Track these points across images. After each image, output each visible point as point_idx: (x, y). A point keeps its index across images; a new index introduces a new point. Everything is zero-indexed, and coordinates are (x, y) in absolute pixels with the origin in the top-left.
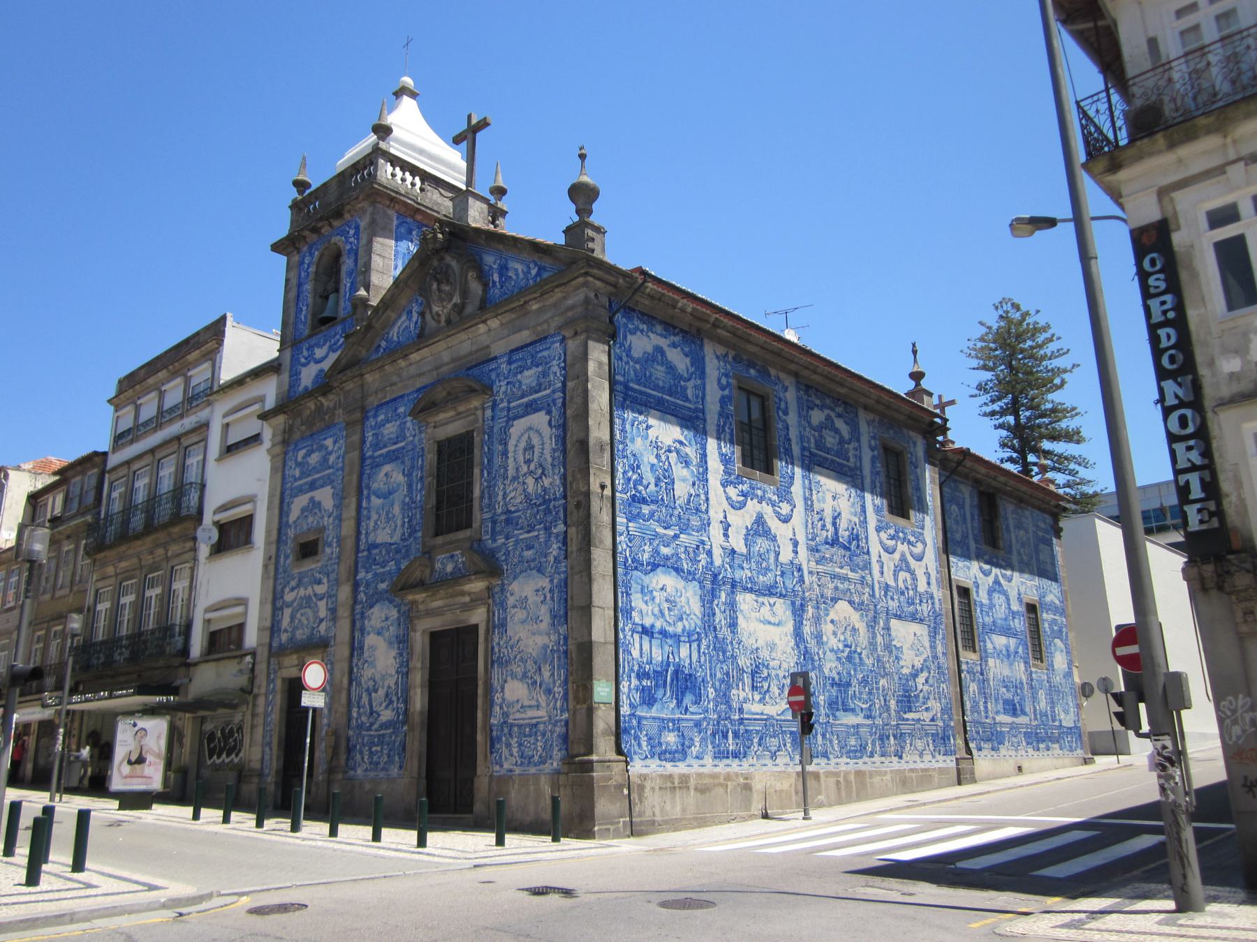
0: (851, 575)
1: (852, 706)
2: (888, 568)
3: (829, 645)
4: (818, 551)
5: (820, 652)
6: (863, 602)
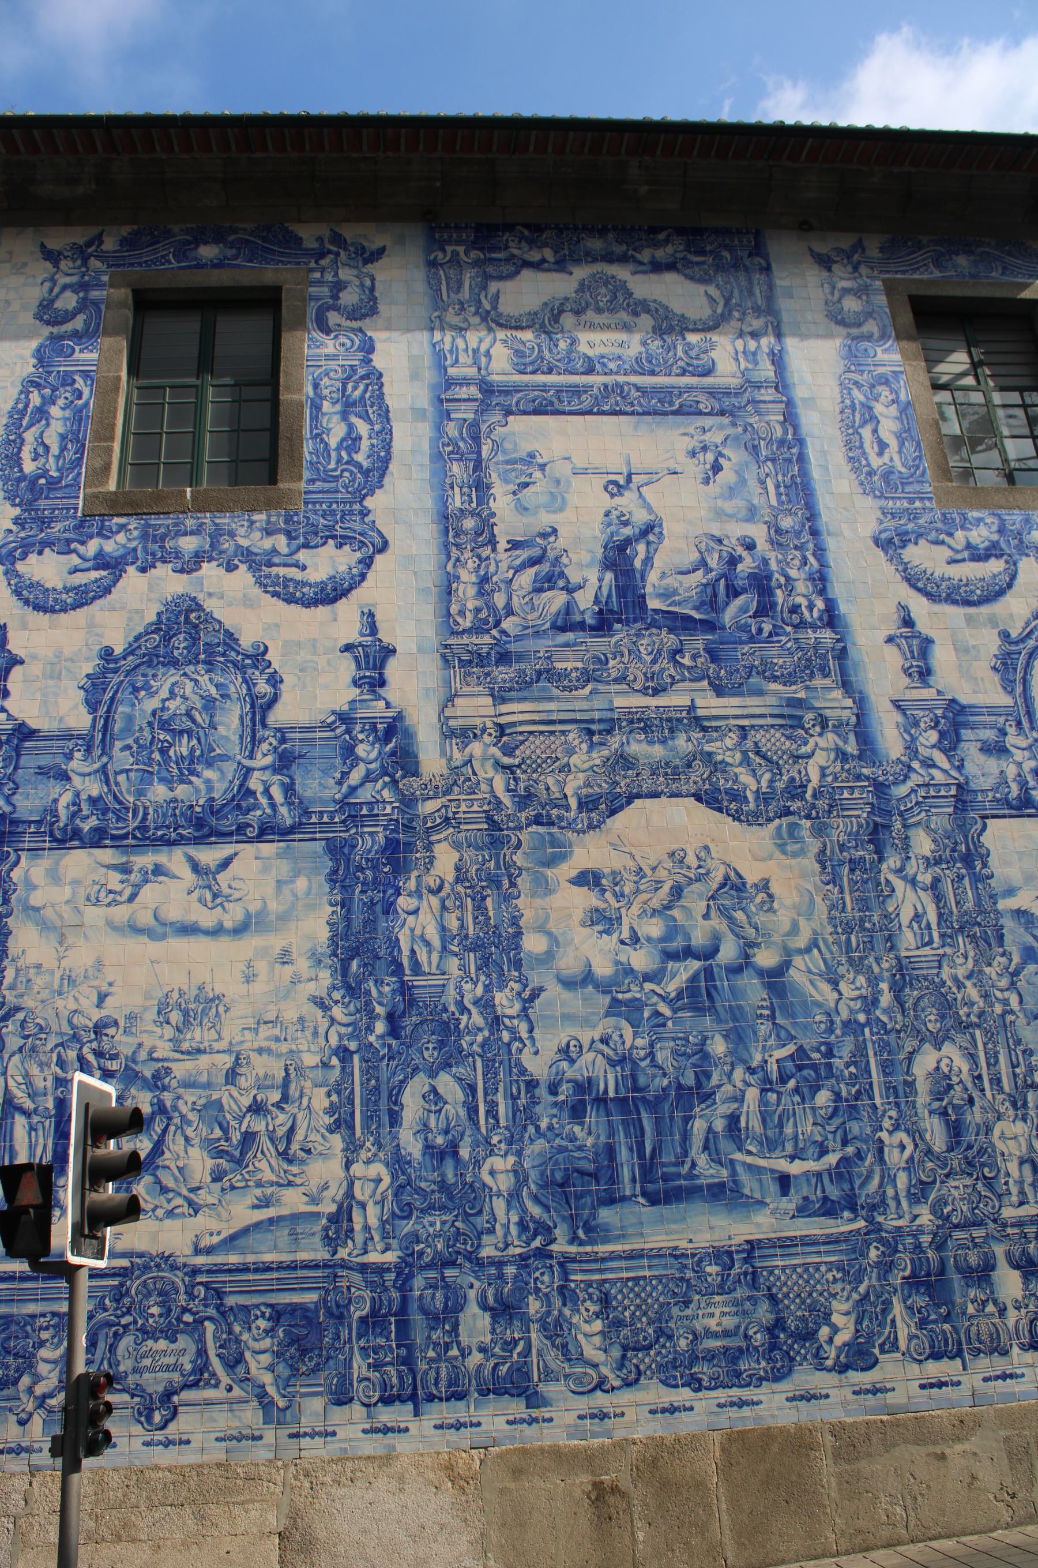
0: (709, 704)
1: (708, 1171)
2: (962, 649)
3: (568, 963)
4: (504, 658)
5: (500, 998)
6: (796, 789)
